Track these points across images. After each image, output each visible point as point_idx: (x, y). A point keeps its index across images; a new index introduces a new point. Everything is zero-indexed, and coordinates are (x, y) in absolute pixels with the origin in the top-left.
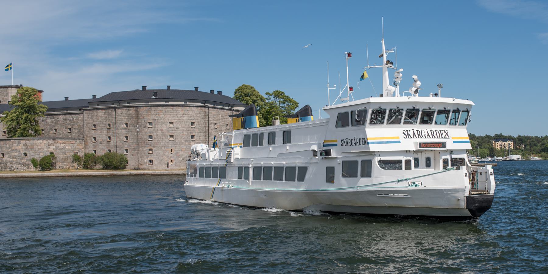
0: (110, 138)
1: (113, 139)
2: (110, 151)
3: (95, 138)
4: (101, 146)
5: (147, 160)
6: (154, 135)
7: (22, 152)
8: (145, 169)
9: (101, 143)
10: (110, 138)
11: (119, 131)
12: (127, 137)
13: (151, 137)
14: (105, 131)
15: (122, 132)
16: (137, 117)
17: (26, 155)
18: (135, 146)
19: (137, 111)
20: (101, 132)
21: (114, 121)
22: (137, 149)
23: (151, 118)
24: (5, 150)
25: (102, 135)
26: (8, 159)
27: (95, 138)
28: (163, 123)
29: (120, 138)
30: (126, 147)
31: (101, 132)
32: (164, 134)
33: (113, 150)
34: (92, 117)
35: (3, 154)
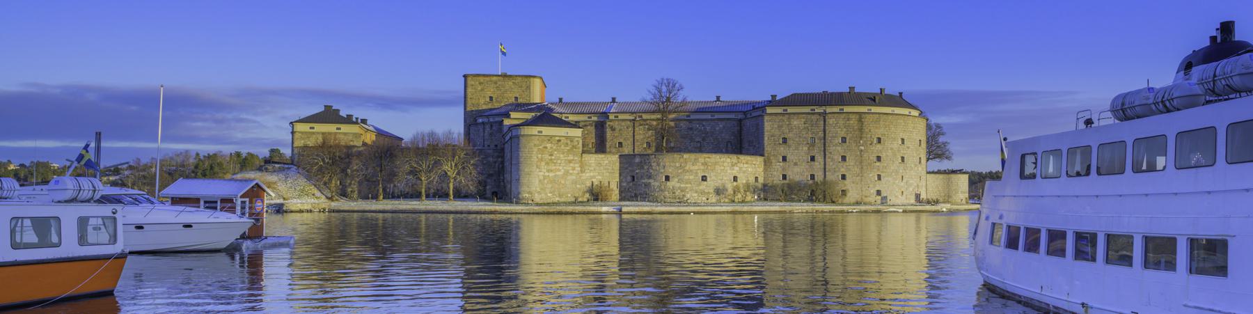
0: (813, 159)
1: (819, 158)
2: (812, 177)
3: (784, 159)
4: (796, 169)
5: (873, 191)
6: (883, 156)
7: (700, 175)
8: (870, 204)
9: (796, 164)
10: (813, 159)
11: (830, 149)
12: (844, 158)
13: (879, 159)
14: (806, 148)
15: (836, 150)
16: (861, 130)
17: (704, 179)
18: (857, 170)
19: (860, 120)
20: (797, 149)
21: (821, 134)
22: (861, 175)
23: (879, 132)
24: (670, 171)
25: (797, 154)
26: (678, 185)
27: (784, 159)
28: (894, 139)
29: (833, 160)
30: (843, 171)
31: (797, 149)
32: (895, 155)
33: (819, 177)
34: (780, 127)
35: (667, 178)
